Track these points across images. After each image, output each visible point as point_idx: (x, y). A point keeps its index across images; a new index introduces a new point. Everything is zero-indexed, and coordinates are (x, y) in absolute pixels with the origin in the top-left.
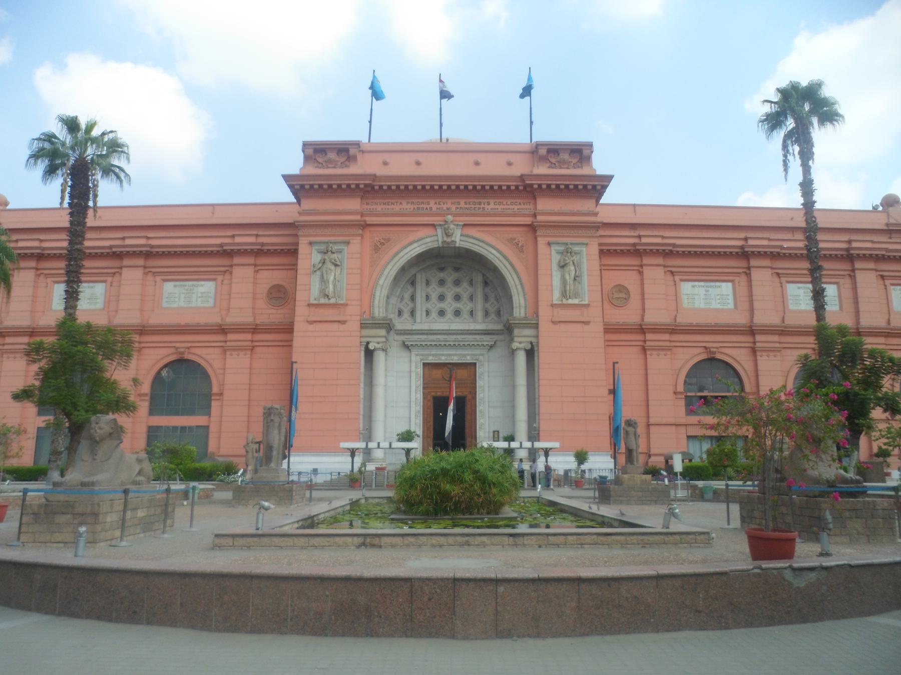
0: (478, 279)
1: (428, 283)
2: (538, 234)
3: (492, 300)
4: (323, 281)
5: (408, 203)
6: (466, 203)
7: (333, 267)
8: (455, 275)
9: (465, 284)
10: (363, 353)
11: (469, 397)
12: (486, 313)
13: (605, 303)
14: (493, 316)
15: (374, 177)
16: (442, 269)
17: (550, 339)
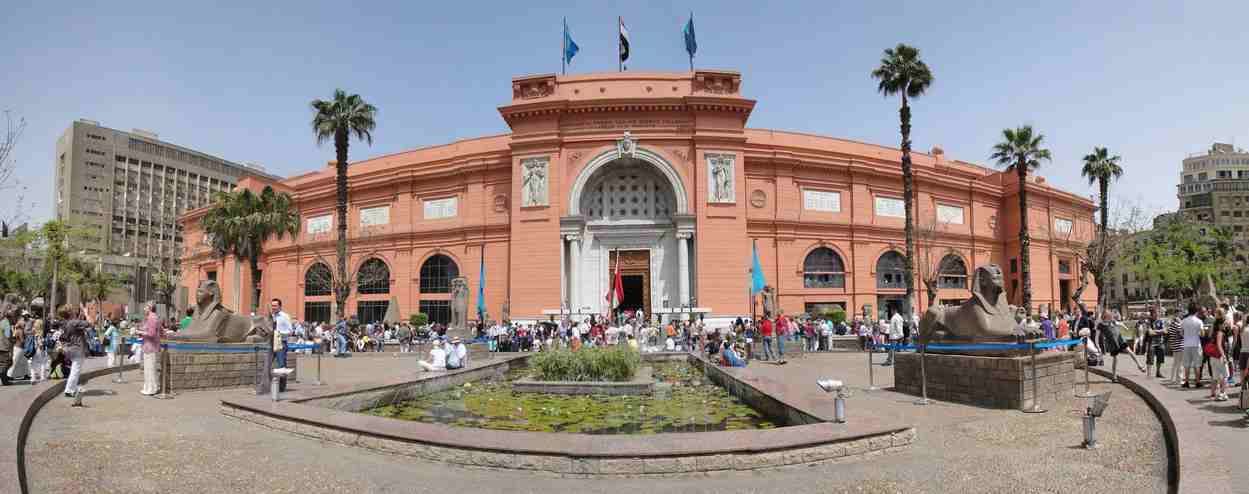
0: (651, 184)
1: (612, 189)
2: (697, 146)
3: (662, 202)
4: (531, 189)
5: (595, 123)
6: (641, 122)
7: (538, 178)
8: (633, 182)
9: (640, 189)
10: (562, 244)
11: (645, 276)
12: (657, 212)
13: (748, 204)
14: (662, 214)
15: (567, 103)
16: (622, 178)
17: (709, 236)
